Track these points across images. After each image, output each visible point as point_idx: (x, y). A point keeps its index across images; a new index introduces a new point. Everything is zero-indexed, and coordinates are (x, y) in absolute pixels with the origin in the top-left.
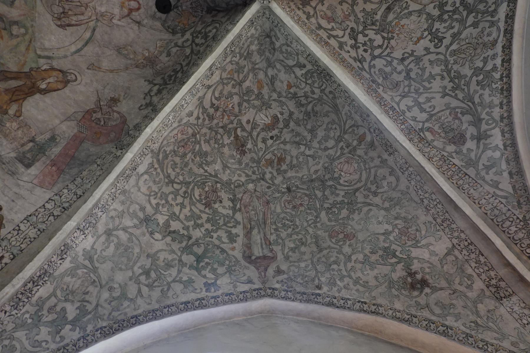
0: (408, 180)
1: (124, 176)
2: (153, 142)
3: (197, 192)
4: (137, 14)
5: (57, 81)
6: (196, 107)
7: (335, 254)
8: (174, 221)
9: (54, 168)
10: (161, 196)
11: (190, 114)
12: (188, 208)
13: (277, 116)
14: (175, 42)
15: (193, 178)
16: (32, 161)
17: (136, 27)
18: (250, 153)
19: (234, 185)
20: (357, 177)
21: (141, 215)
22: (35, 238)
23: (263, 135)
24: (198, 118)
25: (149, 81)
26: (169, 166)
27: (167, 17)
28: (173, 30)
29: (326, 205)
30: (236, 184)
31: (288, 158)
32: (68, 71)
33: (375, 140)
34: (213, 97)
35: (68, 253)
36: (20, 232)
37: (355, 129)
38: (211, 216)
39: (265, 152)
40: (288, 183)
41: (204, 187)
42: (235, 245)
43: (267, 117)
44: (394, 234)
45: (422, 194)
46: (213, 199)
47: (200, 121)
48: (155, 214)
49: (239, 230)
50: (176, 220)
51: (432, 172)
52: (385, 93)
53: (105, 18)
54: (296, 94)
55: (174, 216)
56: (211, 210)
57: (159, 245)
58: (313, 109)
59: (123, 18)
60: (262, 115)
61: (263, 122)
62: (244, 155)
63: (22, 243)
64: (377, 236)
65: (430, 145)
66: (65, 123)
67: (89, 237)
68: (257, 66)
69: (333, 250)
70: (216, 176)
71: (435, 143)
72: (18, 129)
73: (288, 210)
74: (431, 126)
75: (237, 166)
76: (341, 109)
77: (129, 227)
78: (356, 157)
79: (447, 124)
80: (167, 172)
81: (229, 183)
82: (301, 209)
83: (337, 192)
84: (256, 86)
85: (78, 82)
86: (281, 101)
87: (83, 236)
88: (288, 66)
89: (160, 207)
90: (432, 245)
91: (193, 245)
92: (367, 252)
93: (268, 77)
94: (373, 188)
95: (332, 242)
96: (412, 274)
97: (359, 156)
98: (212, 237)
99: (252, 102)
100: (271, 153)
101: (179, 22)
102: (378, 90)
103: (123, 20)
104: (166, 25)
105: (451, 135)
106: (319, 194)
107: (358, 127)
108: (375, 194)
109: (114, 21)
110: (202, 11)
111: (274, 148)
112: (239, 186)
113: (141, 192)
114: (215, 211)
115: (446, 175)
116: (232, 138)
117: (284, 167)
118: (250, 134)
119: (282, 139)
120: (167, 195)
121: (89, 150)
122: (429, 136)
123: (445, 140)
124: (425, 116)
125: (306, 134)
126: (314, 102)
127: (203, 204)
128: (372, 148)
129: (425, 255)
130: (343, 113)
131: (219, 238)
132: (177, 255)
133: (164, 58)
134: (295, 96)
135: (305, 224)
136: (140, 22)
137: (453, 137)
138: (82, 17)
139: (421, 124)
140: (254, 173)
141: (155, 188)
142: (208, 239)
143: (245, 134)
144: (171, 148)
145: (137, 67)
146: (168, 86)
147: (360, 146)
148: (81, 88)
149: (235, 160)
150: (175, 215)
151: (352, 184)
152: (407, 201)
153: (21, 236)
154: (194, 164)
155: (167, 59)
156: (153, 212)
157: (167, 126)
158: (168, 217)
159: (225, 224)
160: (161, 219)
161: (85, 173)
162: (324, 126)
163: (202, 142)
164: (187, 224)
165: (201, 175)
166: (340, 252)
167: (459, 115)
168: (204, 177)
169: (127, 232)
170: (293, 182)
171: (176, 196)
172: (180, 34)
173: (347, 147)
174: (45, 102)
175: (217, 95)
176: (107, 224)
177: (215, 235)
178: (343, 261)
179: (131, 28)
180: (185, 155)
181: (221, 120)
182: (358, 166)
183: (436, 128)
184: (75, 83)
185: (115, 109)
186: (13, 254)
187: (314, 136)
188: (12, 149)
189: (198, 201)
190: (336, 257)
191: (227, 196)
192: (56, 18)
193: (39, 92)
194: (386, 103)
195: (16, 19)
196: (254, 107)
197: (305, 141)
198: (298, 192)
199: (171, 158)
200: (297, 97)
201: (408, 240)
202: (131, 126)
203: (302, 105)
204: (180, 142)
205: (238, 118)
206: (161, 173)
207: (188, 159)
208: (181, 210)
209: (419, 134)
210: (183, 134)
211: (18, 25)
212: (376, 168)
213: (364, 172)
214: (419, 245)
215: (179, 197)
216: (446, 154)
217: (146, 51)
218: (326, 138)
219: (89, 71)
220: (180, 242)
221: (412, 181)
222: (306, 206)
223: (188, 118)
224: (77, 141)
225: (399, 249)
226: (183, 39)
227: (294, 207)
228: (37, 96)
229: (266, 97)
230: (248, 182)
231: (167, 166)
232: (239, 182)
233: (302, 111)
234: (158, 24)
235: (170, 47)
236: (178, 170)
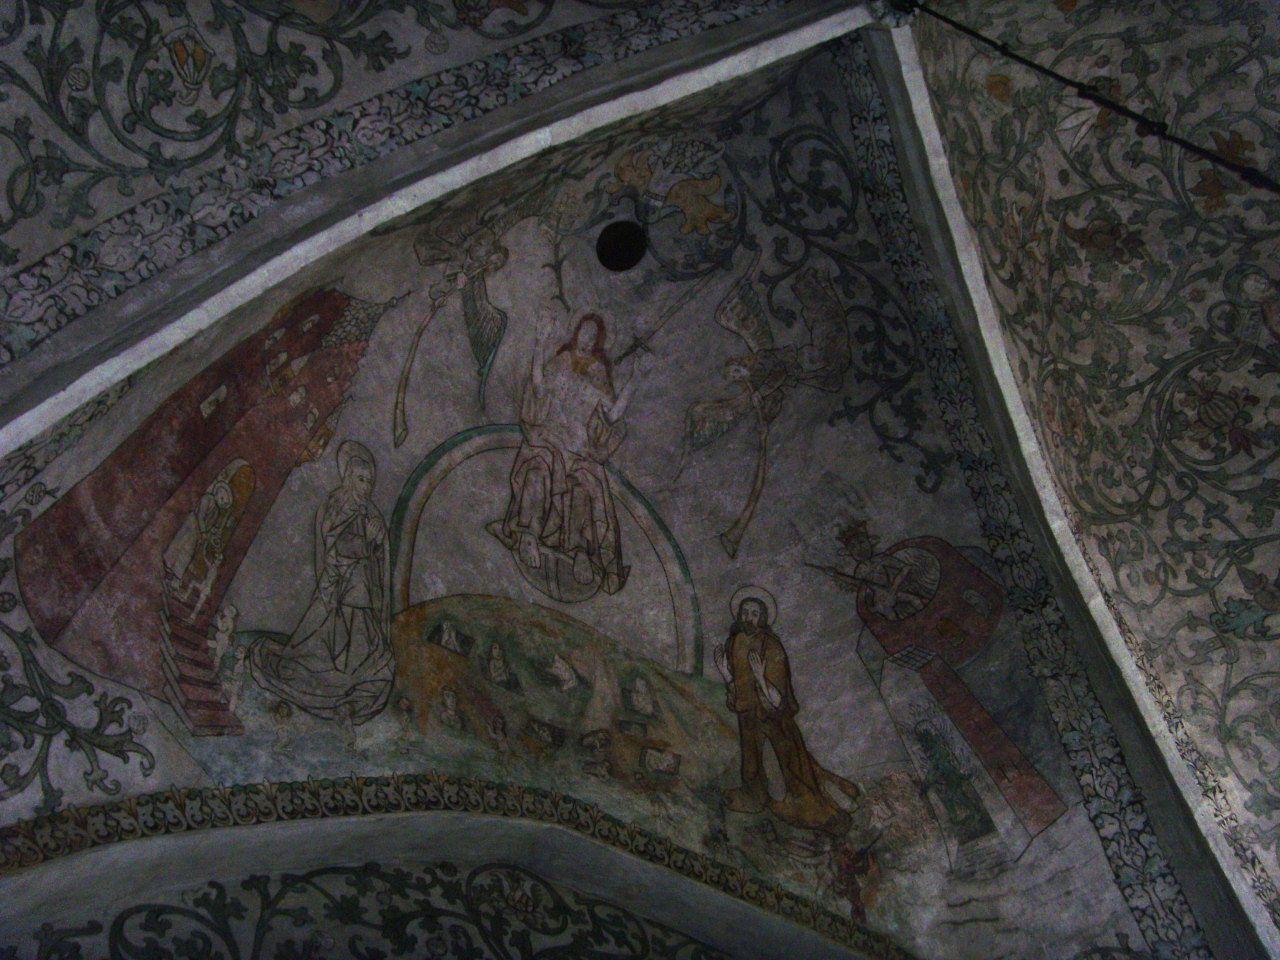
3: (1193, 450)
4: (611, 336)
5: (763, 657)
6: (1014, 341)
8: (1250, 558)
9: (1010, 775)
10: (1173, 555)
12: (1230, 501)
14: (755, 275)
16: (979, 811)
17: (647, 361)
18: (1146, 223)
19: (1220, 330)
21: (1205, 634)
22: (1180, 892)
23: (1116, 150)
25: (839, 415)
26: (1107, 491)
27: (655, 254)
28: (706, 257)
30: (1221, 324)
31: (1245, 127)
32: (735, 612)
35: (1245, 844)
36: (1150, 911)
39: (1168, 175)
41: (1181, 418)
43: (1079, 109)
46: (1231, 414)
48: (1212, 595)
50: (1250, 549)
53: (603, 440)
56: (1265, 442)
59: (611, 385)
60: (1068, 124)
61: (1084, 129)
62: (1143, 243)
63: (1180, 921)
66: (885, 692)
67: (1223, 781)
70: (1164, 366)
72: (889, 807)
75: (1165, 285)
80: (1120, 506)
81: (1204, 341)
85: (768, 602)
86: (1073, 47)
87: (1219, 796)
89: (1201, 572)
100: (1187, 164)
101: (695, 229)
103: (617, 385)
104: (679, 268)
109: (614, 416)
110: (708, 147)
112: (1232, 320)
116: (1082, 255)
118: (1096, 189)
120: (1174, 539)
121: (991, 674)
125: (1219, 33)
127: (1234, 453)
133: (787, 337)
136: (636, 339)
138: (599, 506)
140: (1215, 251)
143: (1088, 206)
144: (1073, 464)
145: (769, 419)
146: (913, 384)
148: (787, 602)
149: (1142, 281)
153: (1162, 914)
155: (798, 327)
156: (1207, 598)
158: (1233, 569)
160: (1233, 588)
161: (1059, 716)
165: (1146, 406)
168: (1154, 402)
171: (1184, 516)
172: (740, 248)
174: (819, 714)
179: (646, 374)
180: (1089, 429)
184: (771, 610)
185: (882, 546)
186: (1198, 948)
188: (939, 840)
189: (1215, 461)
191: (1243, 371)
192: (603, 579)
193: (792, 716)
195: (618, 691)
196: (1038, 137)
202: (977, 541)
205: (1044, 207)
207: (1098, 426)
208: (1226, 521)
211: (630, 692)
215: (1189, 508)
217: (734, 367)
219: (742, 555)
224: (947, 686)
226: (767, 254)
228: (804, 724)
230: (1232, 287)
231: (1107, 498)
232: (1216, 312)
234: (663, 289)
235: (763, 300)
236: (1118, 471)
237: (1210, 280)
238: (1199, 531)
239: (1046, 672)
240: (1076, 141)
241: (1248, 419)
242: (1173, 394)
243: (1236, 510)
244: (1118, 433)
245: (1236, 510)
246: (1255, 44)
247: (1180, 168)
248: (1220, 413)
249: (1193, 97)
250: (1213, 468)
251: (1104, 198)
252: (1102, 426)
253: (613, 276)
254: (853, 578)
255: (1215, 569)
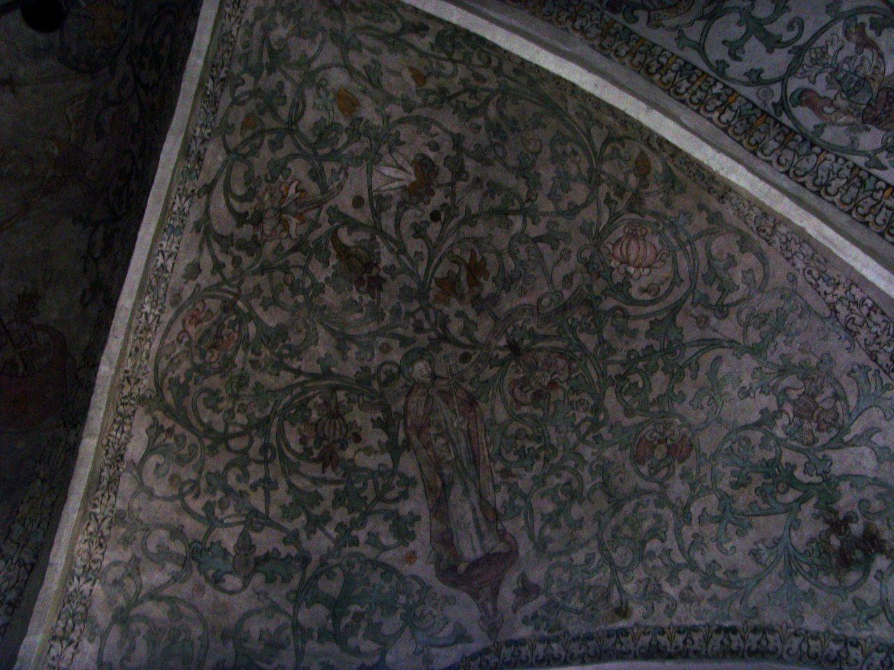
0: (788, 259)
1: (102, 485)
2: (133, 381)
3: (293, 438)
7: (652, 508)
8: (257, 531)
10: (209, 484)
11: (195, 269)
12: (283, 486)
13: (425, 157)
15: (271, 404)
18: (393, 278)
19: (379, 380)
20: (668, 270)
21: (178, 548)
23: (410, 216)
24: (218, 267)
29: (612, 370)
30: (383, 377)
31: (492, 259)
33: (674, 168)
34: (231, 200)
37: (619, 146)
38: (341, 487)
39: (430, 260)
40: (509, 331)
41: (307, 414)
42: (412, 546)
43: (401, 168)
44: (784, 420)
45: (829, 290)
47: (229, 269)
48: (209, 532)
49: (416, 504)
50: (263, 525)
51: (825, 238)
52: (657, 27)
54: (443, 91)
55: (255, 520)
57: (241, 603)
58: (501, 114)
60: (387, 171)
61: (397, 184)
62: (380, 289)
64: (742, 433)
65: (813, 145)
68: (315, 65)
69: (646, 497)
70: (327, 373)
71: (828, 135)
73: (525, 410)
74: (805, 83)
75: (373, 326)
76: (562, 105)
77: (162, 587)
78: (648, 218)
79: (846, 67)
80: (202, 424)
81: (364, 379)
82: (558, 394)
83: (632, 325)
84: (337, 111)
86: (418, 119)
87: (71, 649)
88: (388, 35)
89: (217, 511)
90: (879, 430)
91: (316, 577)
92: (724, 484)
93: (359, 73)
94: (715, 295)
95: (642, 475)
96: (838, 525)
97: (655, 214)
98: (355, 542)
99: (345, 152)
102: (636, 27)
105: (863, 98)
106: (590, 341)
107: (620, 139)
108: (722, 310)
111: (450, 242)
112: (392, 378)
113: (158, 498)
114: (351, 470)
115: (874, 228)
116: (333, 261)
117: (488, 287)
118: (376, 229)
119: (462, 209)
120: (222, 476)
122: (806, 117)
123: (852, 120)
124: (782, 57)
125: (511, 181)
126: (495, 99)
127: (315, 461)
128: (677, 188)
129: (864, 462)
130: (572, 113)
131: (373, 539)
132: (286, 613)
134: (444, 96)
135: (573, 438)
137: (869, 105)
139: (777, 88)
140: (419, 328)
141: (188, 474)
142: (347, 550)
143: (363, 236)
144: (186, 365)
147: (646, 186)
149: (360, 311)
150: (257, 517)
151: (662, 292)
152: (800, 316)
154: (263, 370)
156: (204, 529)
157: (149, 330)
158: (242, 527)
159: (380, 498)
160: (228, 538)
161: (24, 509)
162: (546, 153)
163: (259, 311)
164: (290, 526)
165: (290, 387)
166: (663, 500)
167: (870, 33)
168: (298, 390)
169: (160, 599)
170: (520, 323)
171: (243, 468)
173: (620, 194)
175: (239, 190)
176: (110, 601)
177: (362, 535)
178: (672, 524)
180: (228, 362)
181: (285, 234)
182: (660, 242)
183: (821, 87)
185: (35, 320)
187: (534, 183)
190: (655, 516)
191: (369, 416)
194: (663, 60)
196: (357, 160)
197: (516, 201)
198: (540, 350)
199: (198, 387)
200: (451, 98)
201: (819, 429)
203: (473, 112)
204: (200, 341)
205: (326, 207)
206: (187, 433)
207: (240, 366)
209: (777, 121)
210: (199, 322)
212: (705, 238)
213: (680, 253)
214: (846, 438)
215: (252, 468)
216: (860, 160)
218: (564, 181)
220: (286, 580)
221: (796, 260)
222: (565, 385)
223: (193, 283)
225: (801, 460)
227: (538, 395)
229: (377, 121)
230: (409, 360)
231: (195, 409)
232: (387, 367)
233: (480, 127)
237: (401, 345)
238: (243, 487)
239: (42, 474)
240: (386, 187)
241: (343, 447)
242: (314, 396)
243: (281, 494)
244: (252, 384)
245: (281, 494)
246: (527, 205)
247: (440, 260)
248: (332, 430)
249: (477, 216)
250: (292, 458)
251: (378, 239)
252: (243, 369)
253: (24, 26)
254: (4, 326)
255: (230, 517)
